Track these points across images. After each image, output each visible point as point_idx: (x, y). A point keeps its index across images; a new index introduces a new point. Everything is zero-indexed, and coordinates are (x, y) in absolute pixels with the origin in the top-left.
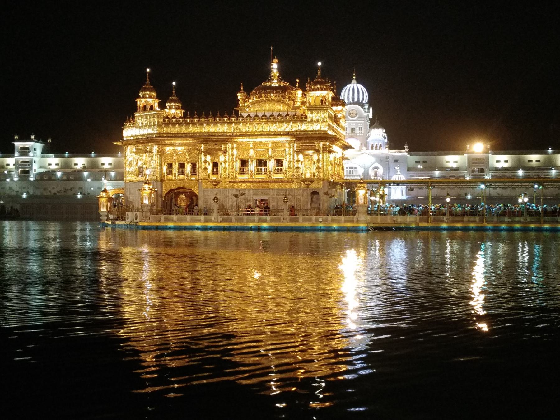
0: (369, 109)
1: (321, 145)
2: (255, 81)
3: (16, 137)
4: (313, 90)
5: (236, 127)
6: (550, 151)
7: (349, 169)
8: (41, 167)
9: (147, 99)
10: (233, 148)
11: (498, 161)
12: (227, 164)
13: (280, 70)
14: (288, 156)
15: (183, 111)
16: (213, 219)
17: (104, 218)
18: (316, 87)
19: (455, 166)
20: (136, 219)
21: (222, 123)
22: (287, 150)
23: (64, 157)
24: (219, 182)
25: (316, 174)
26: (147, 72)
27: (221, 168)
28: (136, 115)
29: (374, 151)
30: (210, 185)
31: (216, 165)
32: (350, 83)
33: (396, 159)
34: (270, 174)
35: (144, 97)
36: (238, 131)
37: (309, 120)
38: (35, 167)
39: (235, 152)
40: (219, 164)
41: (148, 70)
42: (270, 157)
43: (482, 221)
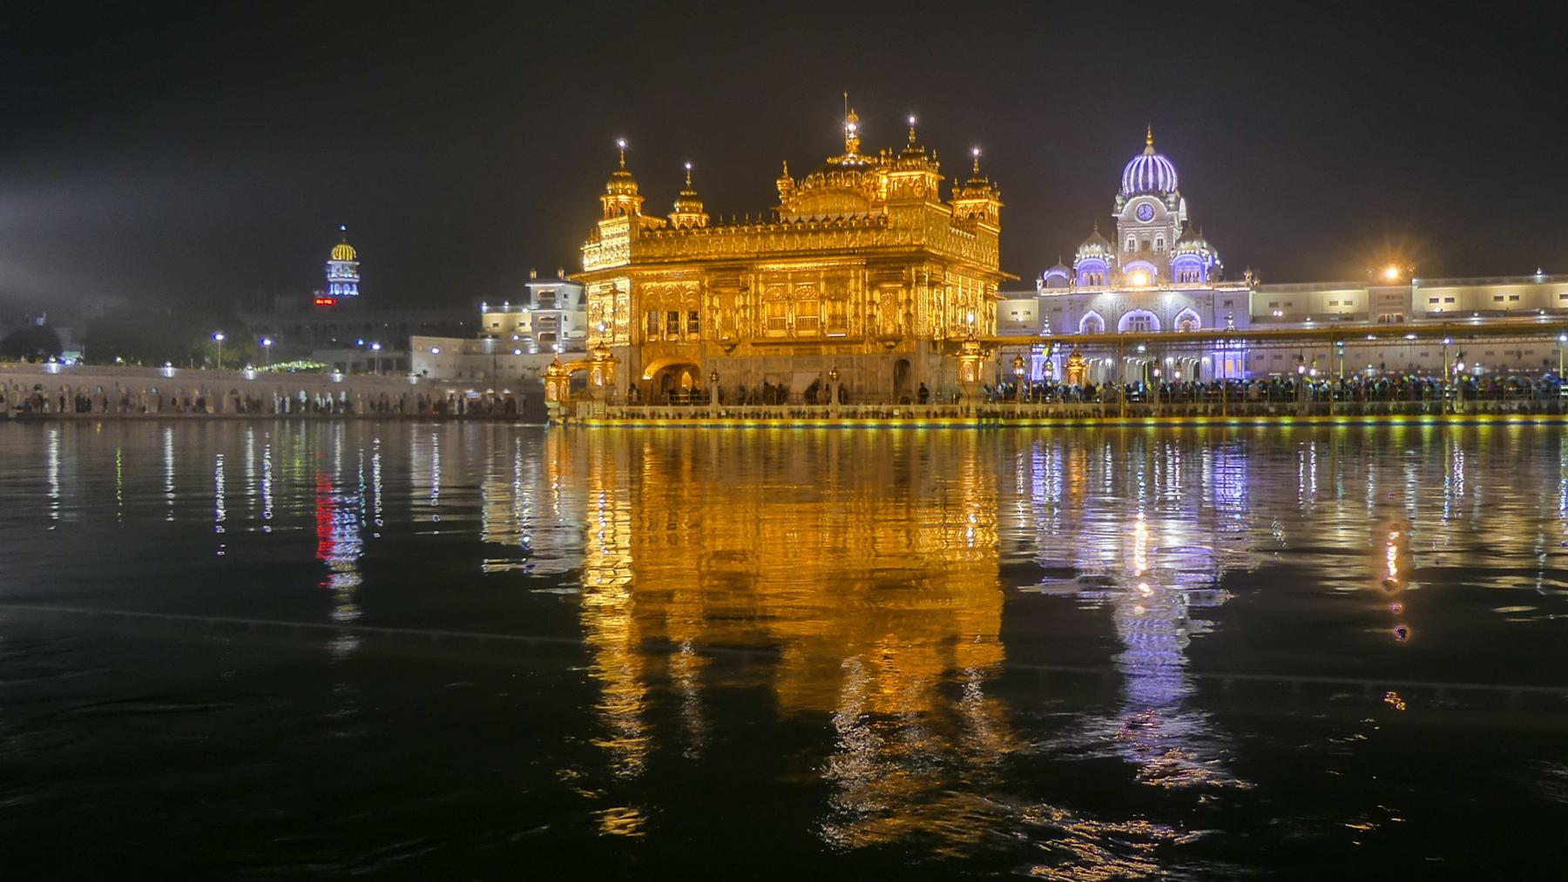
3: (533, 275)
6: (1539, 276)
8: (577, 328)
10: (757, 282)
11: (1432, 301)
15: (705, 217)
19: (1342, 308)
22: (852, 283)
24: (734, 346)
26: (619, 148)
28: (600, 224)
29: (1185, 286)
30: (721, 351)
32: (1141, 152)
35: (615, 193)
37: (891, 225)
38: (565, 327)
39: (761, 289)
41: (622, 143)
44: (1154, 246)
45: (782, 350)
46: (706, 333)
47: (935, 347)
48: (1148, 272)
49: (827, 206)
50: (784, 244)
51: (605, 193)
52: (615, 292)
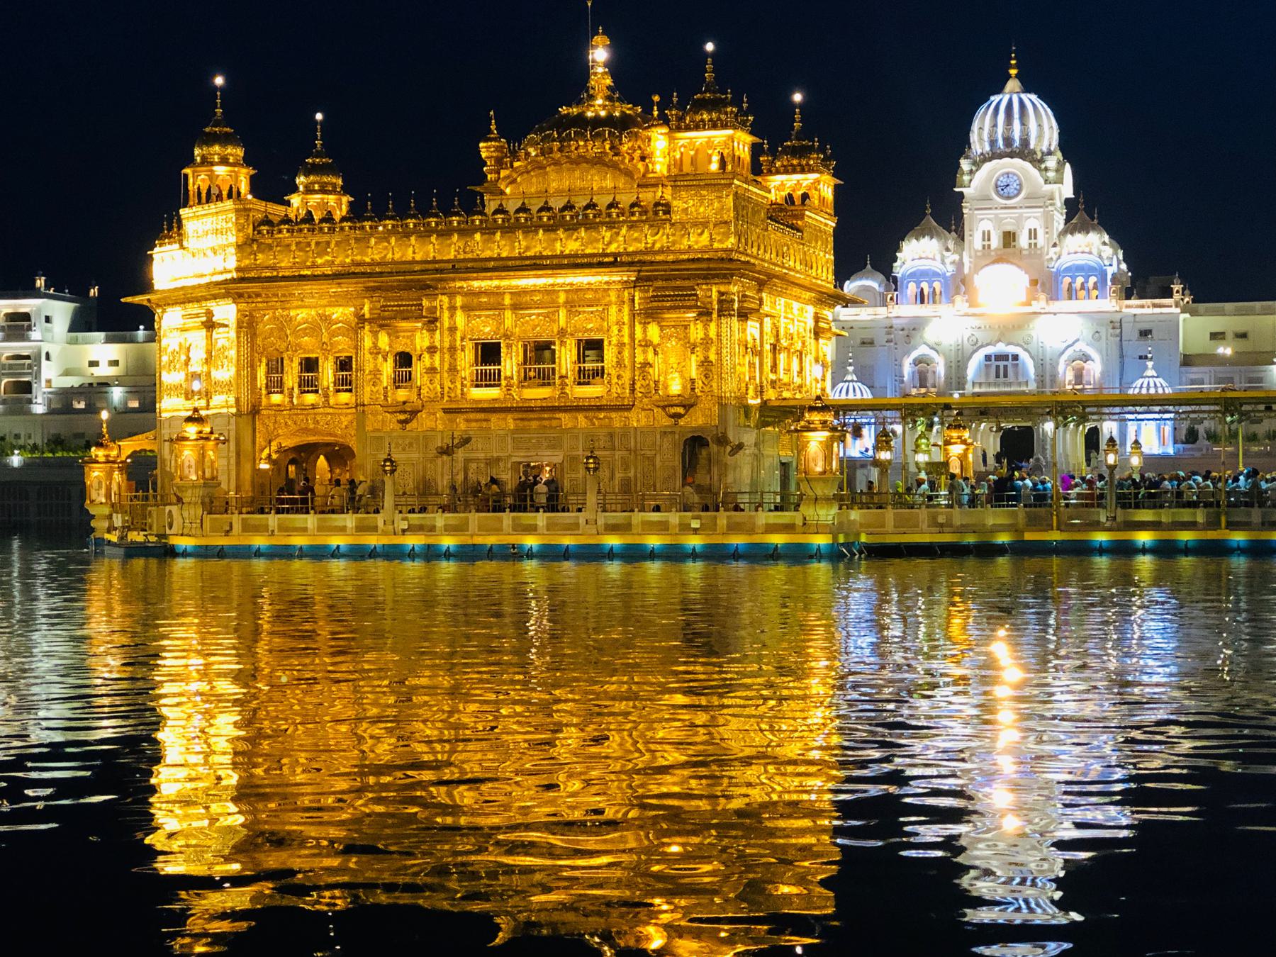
0: (1059, 170)
1: (715, 295)
2: (540, 104)
4: (688, 128)
5: (461, 244)
7: (994, 363)
8: (67, 373)
9: (222, 167)
10: (452, 309)
12: (437, 357)
13: (614, 68)
14: (615, 329)
15: (346, 199)
16: (380, 524)
17: (99, 525)
18: (698, 118)
20: (170, 527)
21: (425, 234)
22: (613, 310)
23: (132, 340)
24: (414, 413)
25: (699, 384)
27: (418, 369)
28: (183, 212)
30: (392, 421)
31: (404, 359)
32: (999, 90)
33: (1145, 326)
34: (564, 385)
35: (206, 162)
36: (470, 256)
37: (675, 217)
38: (50, 372)
39: (460, 319)
40: (414, 359)
42: (562, 333)
43: (1213, 524)
44: (1023, 241)
45: (495, 421)
46: (367, 393)
47: (747, 416)
48: (1020, 281)
49: (559, 183)
50: (500, 247)
51: (190, 161)
52: (210, 325)
